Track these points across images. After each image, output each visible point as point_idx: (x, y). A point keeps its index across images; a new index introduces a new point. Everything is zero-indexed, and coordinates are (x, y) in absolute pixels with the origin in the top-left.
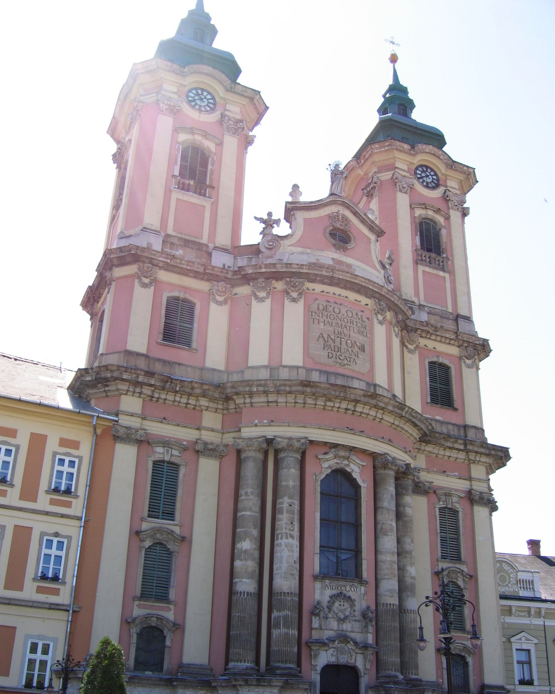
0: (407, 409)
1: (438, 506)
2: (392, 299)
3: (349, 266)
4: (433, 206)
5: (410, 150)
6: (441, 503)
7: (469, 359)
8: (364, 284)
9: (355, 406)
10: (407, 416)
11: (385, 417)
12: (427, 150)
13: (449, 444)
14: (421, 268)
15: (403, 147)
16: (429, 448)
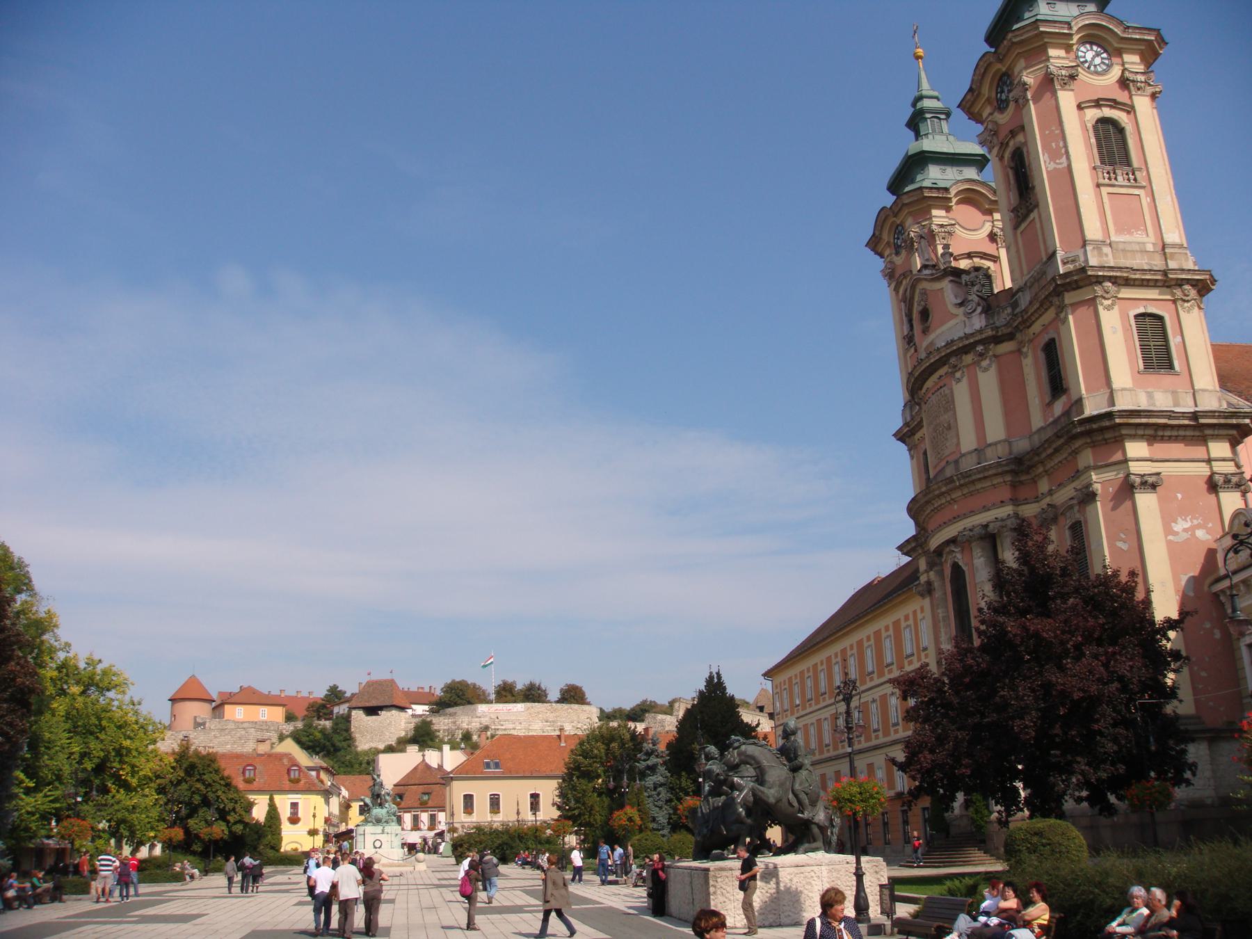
0: (955, 478)
1: (1067, 527)
2: (955, 348)
3: (932, 343)
4: (1006, 136)
5: (973, 94)
6: (1068, 521)
7: (1062, 312)
8: (928, 364)
9: (933, 504)
10: (962, 482)
11: (953, 497)
12: (982, 71)
13: (1044, 455)
14: (1019, 231)
15: (969, 100)
16: (1041, 469)
